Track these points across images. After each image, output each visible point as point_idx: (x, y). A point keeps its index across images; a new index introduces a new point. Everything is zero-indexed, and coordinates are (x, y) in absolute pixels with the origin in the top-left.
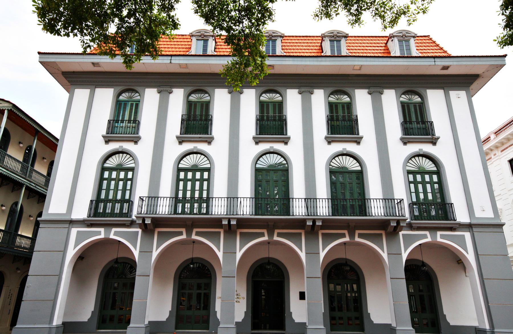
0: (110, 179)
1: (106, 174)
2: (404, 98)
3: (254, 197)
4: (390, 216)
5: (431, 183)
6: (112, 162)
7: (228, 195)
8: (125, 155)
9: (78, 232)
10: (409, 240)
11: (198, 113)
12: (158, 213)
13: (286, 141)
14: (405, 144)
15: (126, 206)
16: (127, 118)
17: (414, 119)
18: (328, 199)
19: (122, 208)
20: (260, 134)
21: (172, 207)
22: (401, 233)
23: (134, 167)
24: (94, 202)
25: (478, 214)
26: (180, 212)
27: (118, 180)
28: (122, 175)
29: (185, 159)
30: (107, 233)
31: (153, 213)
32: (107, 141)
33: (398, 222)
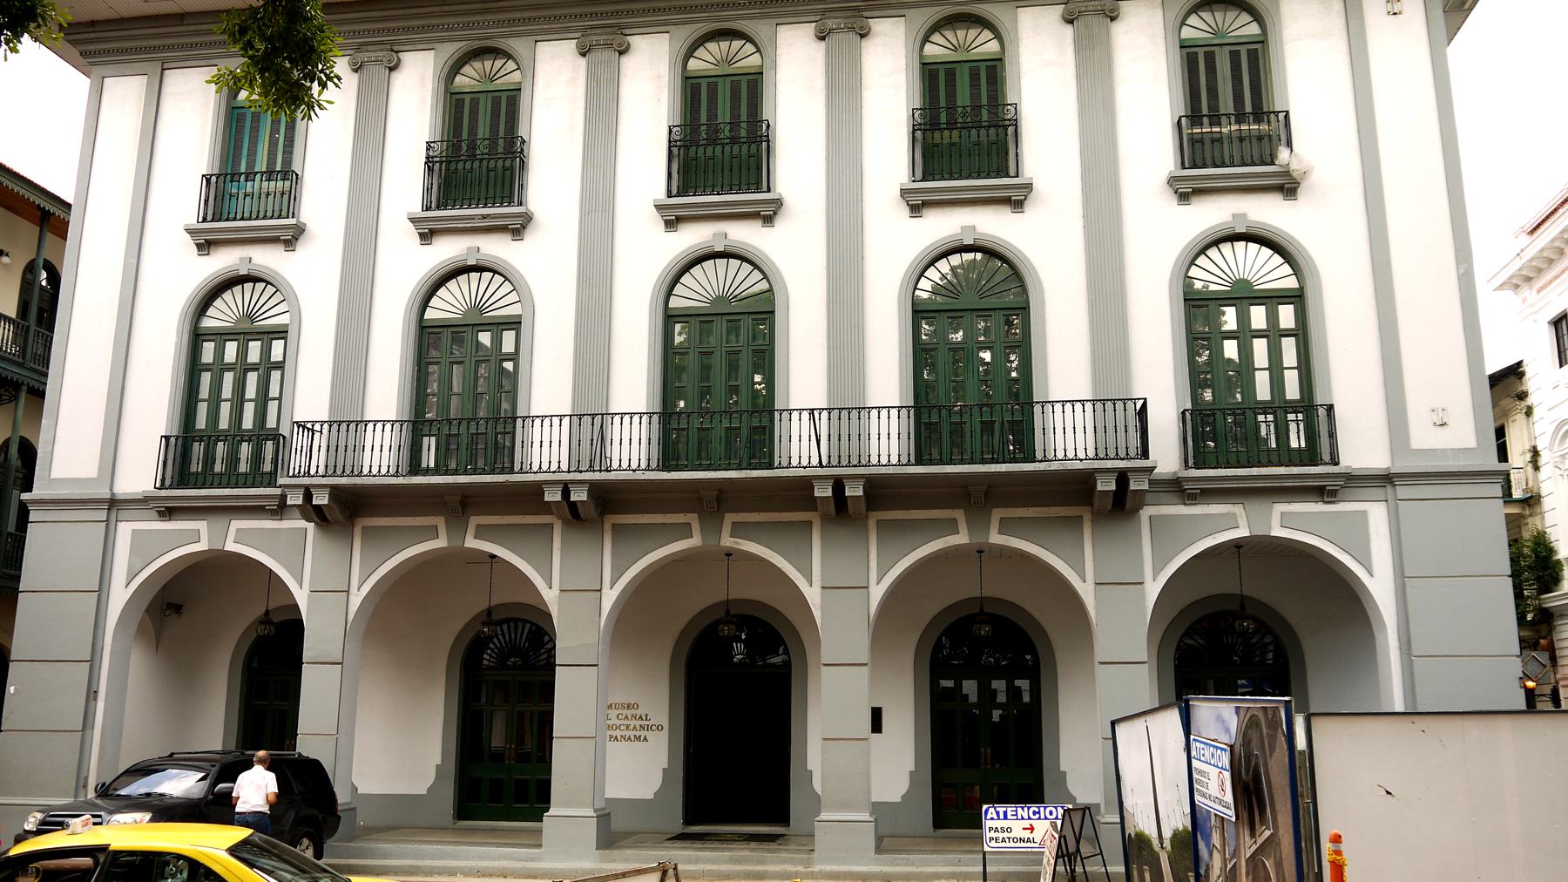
0: (220, 368)
1: (208, 352)
2: (1198, 28)
3: (658, 409)
5: (1273, 334)
6: (221, 315)
8: (248, 286)
12: (366, 471)
13: (768, 214)
14: (1184, 197)
16: (261, 165)
17: (1227, 104)
19: (257, 458)
20: (678, 195)
21: (390, 451)
23: (287, 325)
24: (173, 440)
25: (1423, 436)
26: (432, 465)
27: (243, 368)
28: (254, 351)
29: (442, 292)
31: (335, 472)
32: (206, 246)
33: (1122, 477)
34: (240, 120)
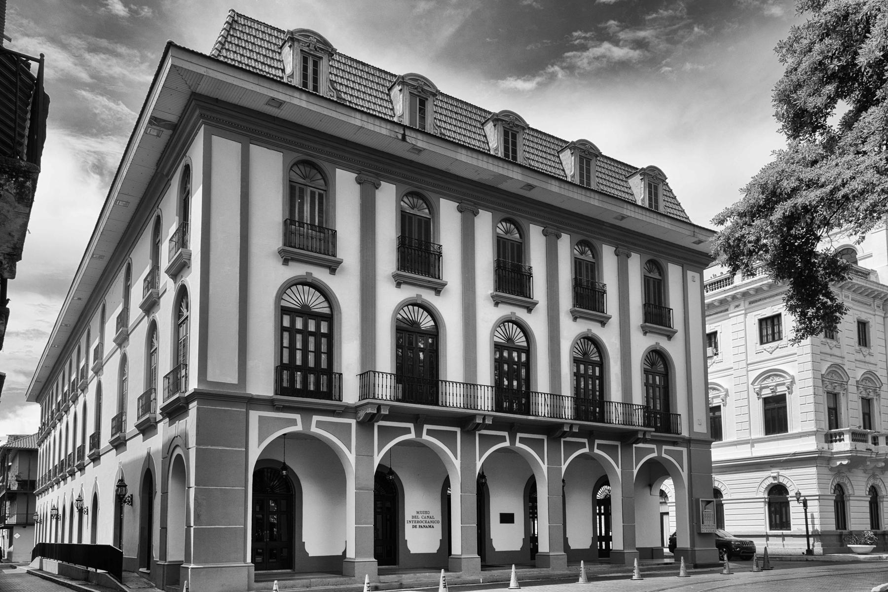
0: (292, 330)
4: (629, 425)
10: (641, 453)
11: (415, 236)
15: (324, 379)
18: (571, 397)
19: (317, 383)
30: (307, 423)
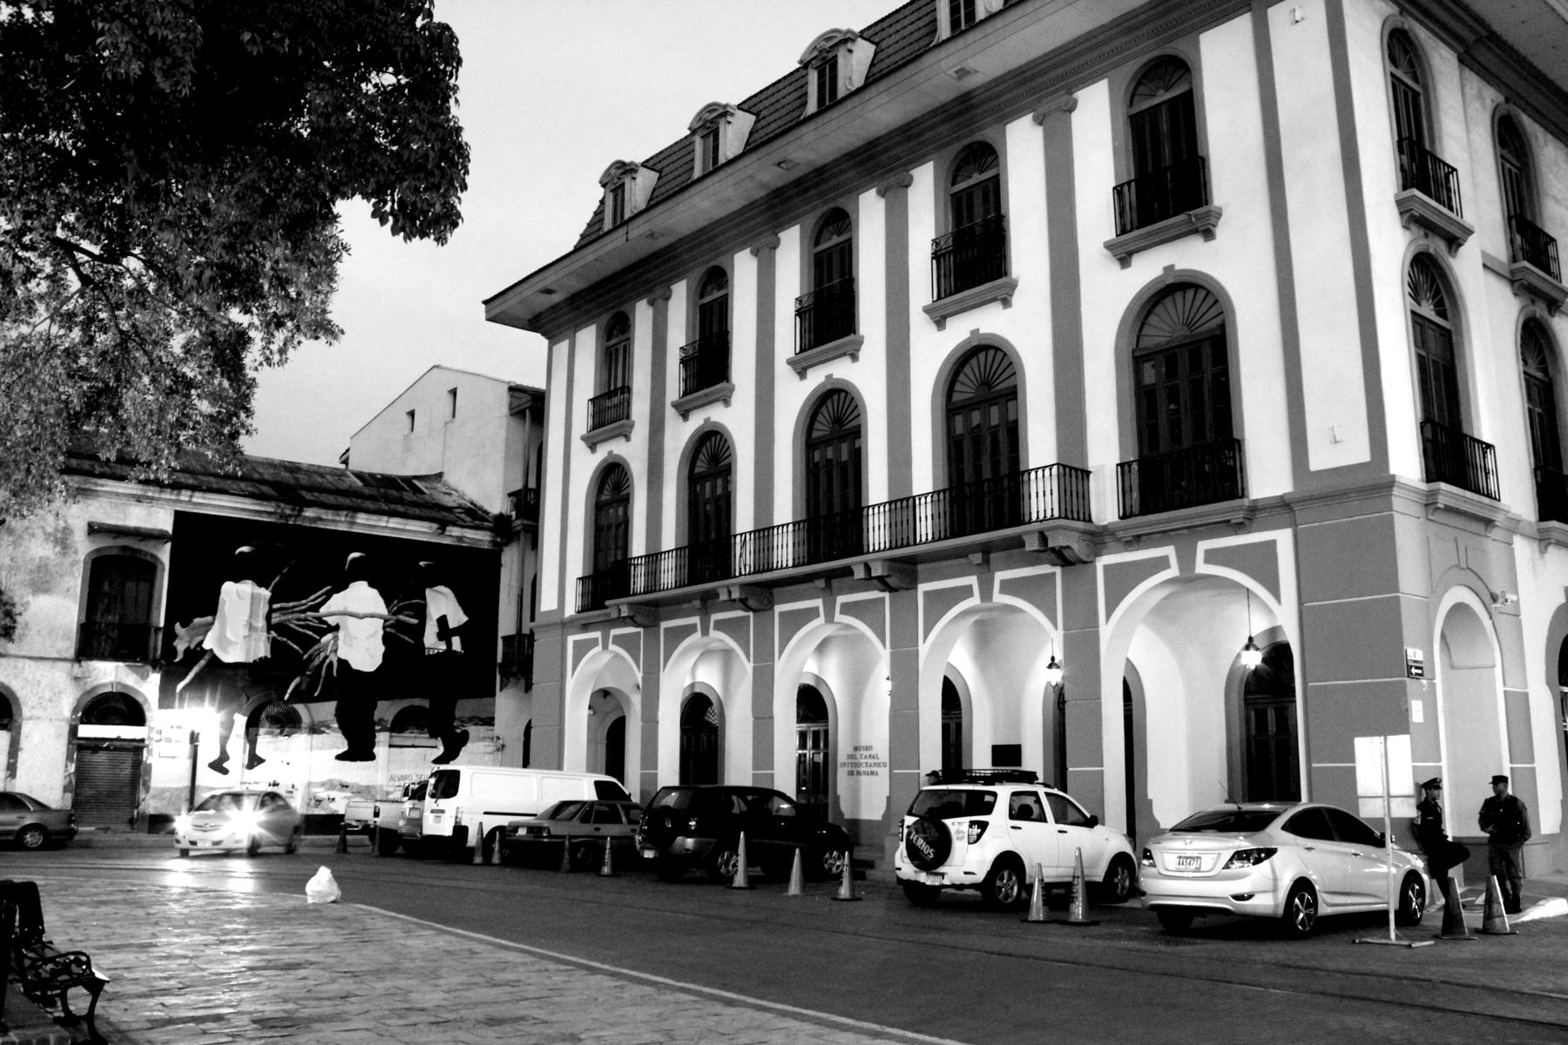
7: (755, 525)
9: (575, 642)
22: (1058, 570)
25: (1320, 459)
34: (611, 354)
